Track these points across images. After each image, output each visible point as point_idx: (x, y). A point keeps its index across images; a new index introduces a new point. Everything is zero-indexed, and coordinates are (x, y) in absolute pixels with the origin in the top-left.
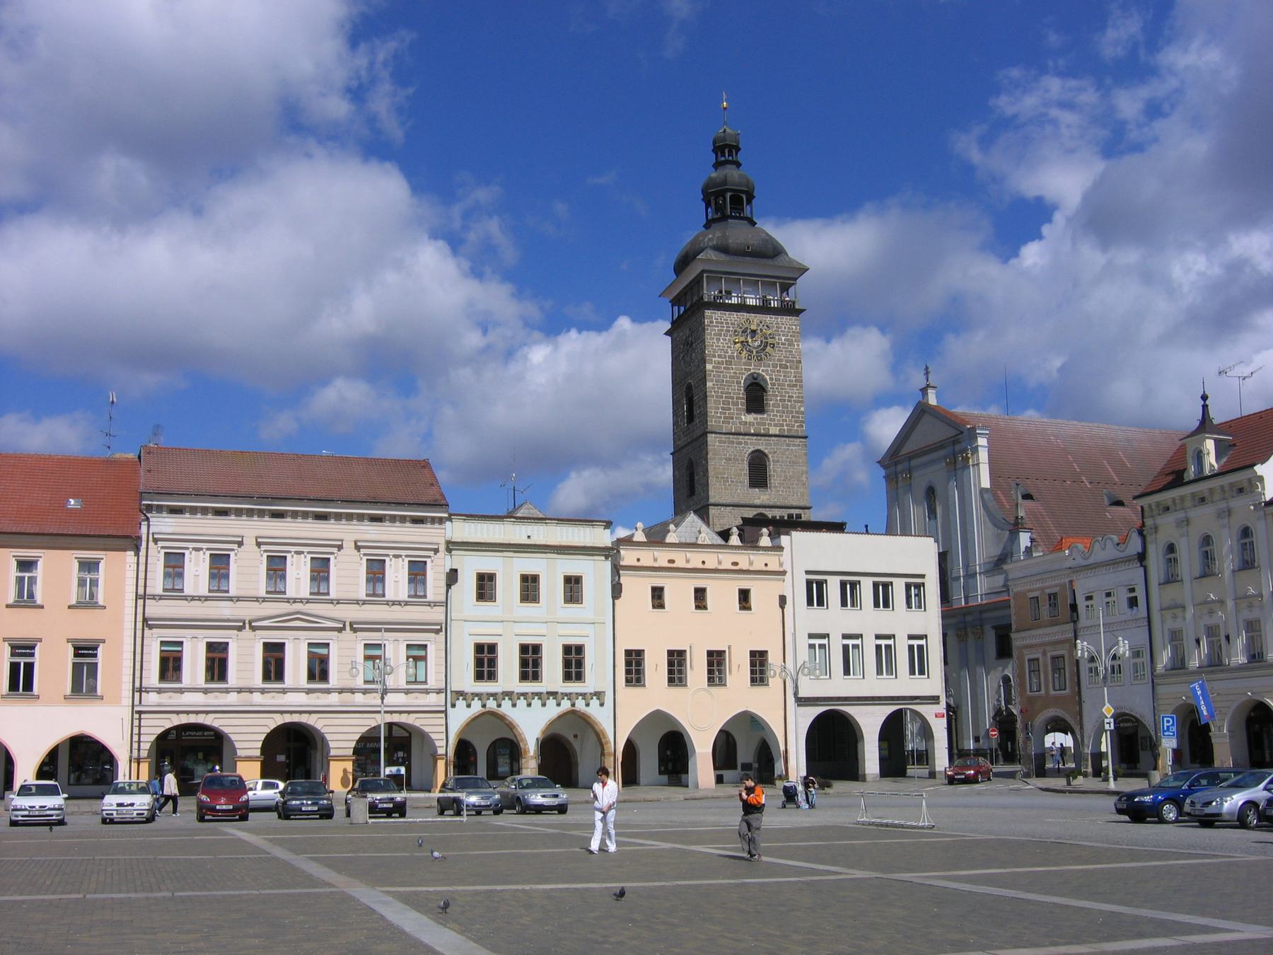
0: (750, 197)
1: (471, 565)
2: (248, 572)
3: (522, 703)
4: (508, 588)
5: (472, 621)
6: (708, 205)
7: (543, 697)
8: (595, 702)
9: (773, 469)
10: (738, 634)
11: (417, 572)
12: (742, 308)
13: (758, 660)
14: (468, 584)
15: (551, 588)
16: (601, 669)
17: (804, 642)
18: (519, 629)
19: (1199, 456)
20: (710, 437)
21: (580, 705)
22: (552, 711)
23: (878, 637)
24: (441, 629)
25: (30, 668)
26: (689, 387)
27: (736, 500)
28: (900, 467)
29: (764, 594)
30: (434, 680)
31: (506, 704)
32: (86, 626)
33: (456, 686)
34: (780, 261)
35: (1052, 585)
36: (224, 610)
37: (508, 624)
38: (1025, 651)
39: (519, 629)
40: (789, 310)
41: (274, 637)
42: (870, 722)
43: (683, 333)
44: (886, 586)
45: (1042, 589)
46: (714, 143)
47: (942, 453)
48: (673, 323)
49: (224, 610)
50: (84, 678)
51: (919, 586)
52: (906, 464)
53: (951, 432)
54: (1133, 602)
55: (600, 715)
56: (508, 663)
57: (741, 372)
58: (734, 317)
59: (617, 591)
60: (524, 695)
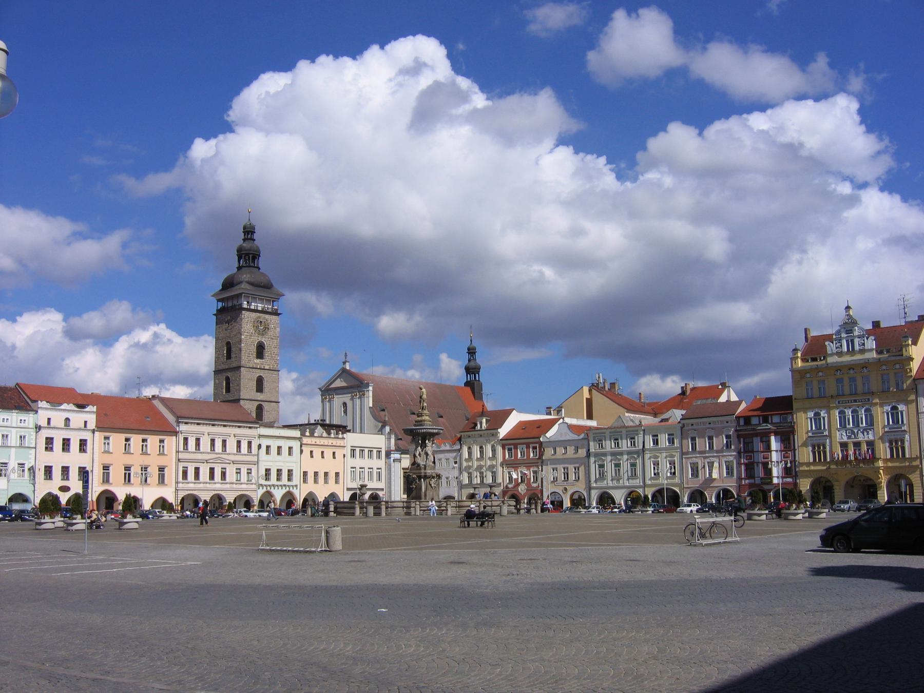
4: (274, 450)
9: (265, 384)
10: (331, 466)
12: (256, 311)
13: (337, 474)
15: (285, 451)
16: (297, 478)
17: (349, 470)
18: (278, 464)
19: (481, 423)
20: (242, 369)
22: (284, 491)
24: (257, 463)
25: (129, 474)
26: (228, 344)
29: (339, 453)
30: (253, 481)
32: (162, 461)
36: (199, 456)
39: (278, 464)
40: (275, 313)
41: (212, 465)
46: (244, 228)
48: (217, 310)
49: (199, 456)
50: (162, 480)
53: (357, 383)
55: (296, 492)
57: (256, 339)
58: (254, 315)
59: (302, 451)
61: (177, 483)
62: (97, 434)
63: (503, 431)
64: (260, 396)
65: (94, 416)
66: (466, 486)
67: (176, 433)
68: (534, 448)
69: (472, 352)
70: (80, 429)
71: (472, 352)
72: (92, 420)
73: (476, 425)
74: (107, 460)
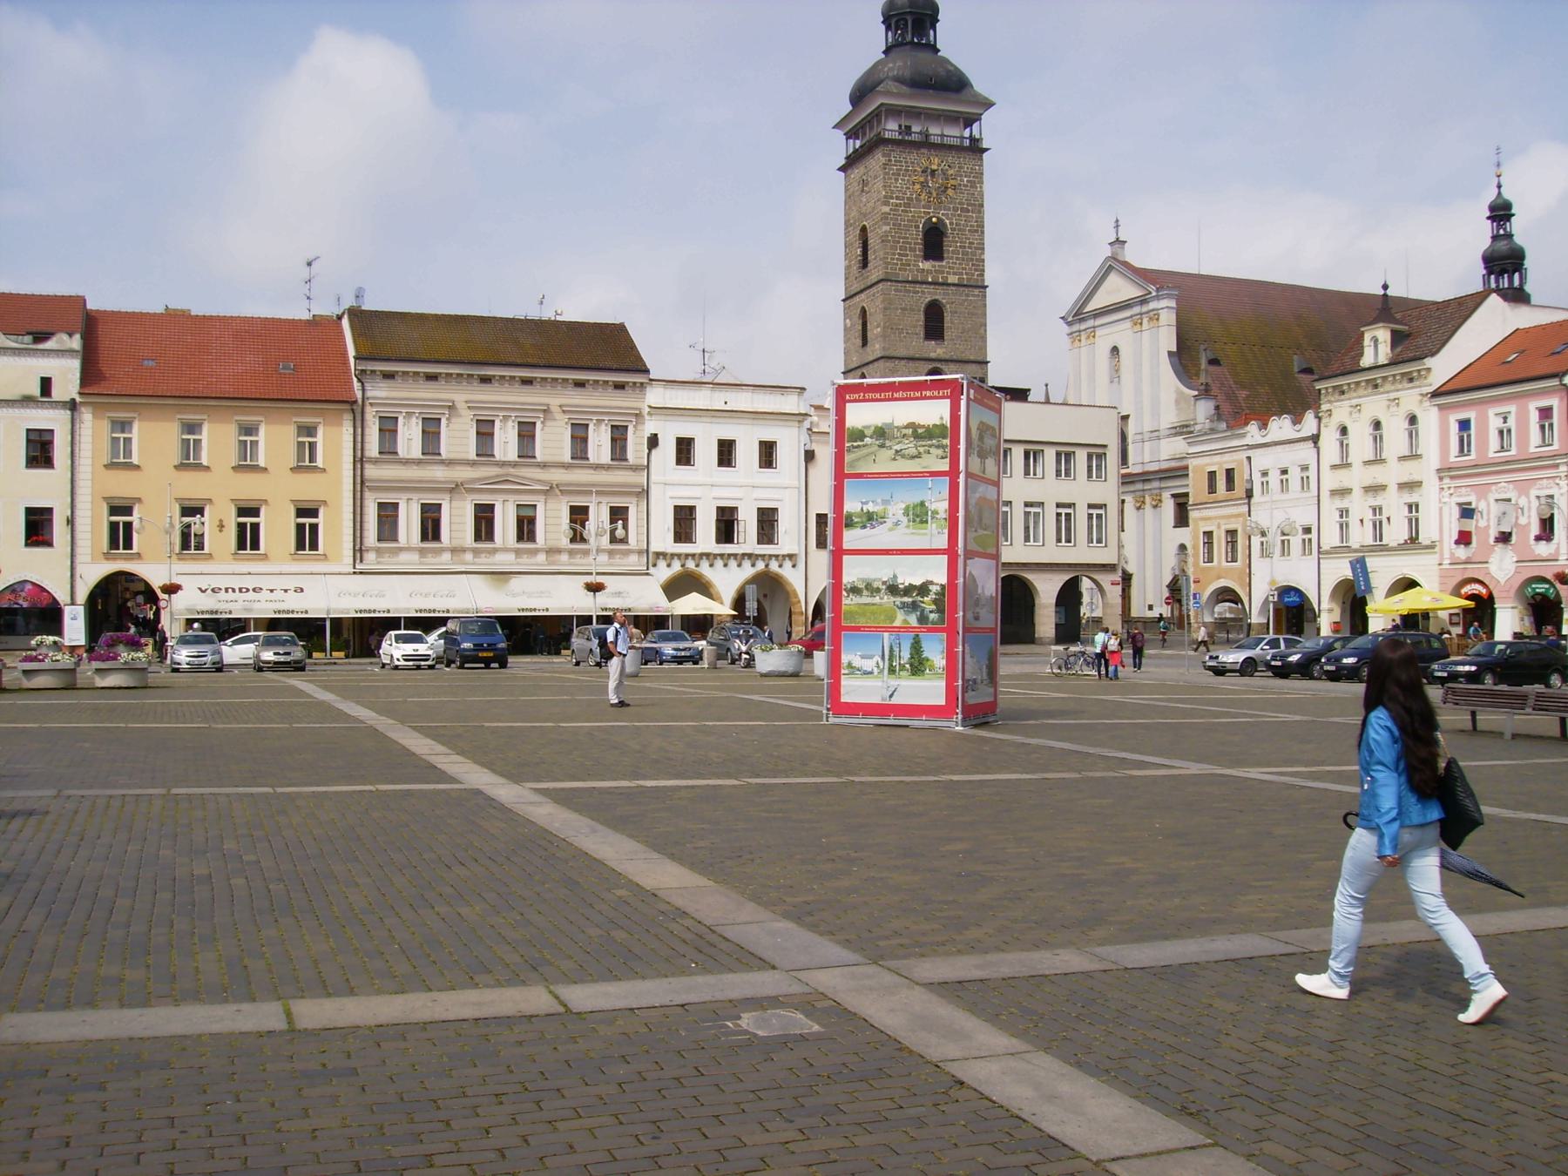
0: (934, 20)
1: (669, 433)
2: (458, 438)
3: (719, 563)
4: (706, 452)
5: (672, 486)
6: (888, 28)
7: (740, 558)
8: (788, 564)
11: (619, 437)
14: (668, 449)
15: (747, 453)
16: (790, 535)
19: (1375, 340)
21: (774, 566)
22: (748, 571)
23: (1058, 505)
27: (911, 353)
28: (1083, 326)
31: (705, 564)
32: (307, 488)
33: (654, 548)
34: (964, 95)
35: (1228, 461)
36: (439, 473)
37: (706, 486)
38: (1201, 523)
41: (485, 499)
42: (1047, 590)
43: (857, 172)
44: (1068, 455)
45: (1220, 464)
47: (1127, 313)
49: (439, 473)
51: (1100, 457)
52: (1090, 323)
54: (1304, 482)
55: (792, 576)
56: (706, 526)
60: (722, 556)
61: (359, 551)
62: (87, 416)
63: (1445, 365)
64: (936, 350)
65: (75, 365)
66: (1335, 551)
67: (355, 409)
68: (1546, 413)
69: (1501, 213)
70: (27, 401)
71: (1501, 213)
72: (67, 374)
73: (1362, 354)
74: (122, 485)
